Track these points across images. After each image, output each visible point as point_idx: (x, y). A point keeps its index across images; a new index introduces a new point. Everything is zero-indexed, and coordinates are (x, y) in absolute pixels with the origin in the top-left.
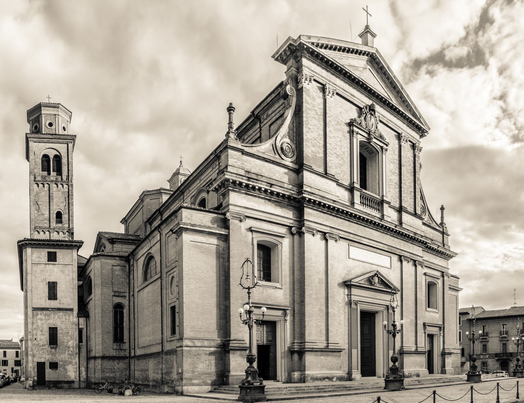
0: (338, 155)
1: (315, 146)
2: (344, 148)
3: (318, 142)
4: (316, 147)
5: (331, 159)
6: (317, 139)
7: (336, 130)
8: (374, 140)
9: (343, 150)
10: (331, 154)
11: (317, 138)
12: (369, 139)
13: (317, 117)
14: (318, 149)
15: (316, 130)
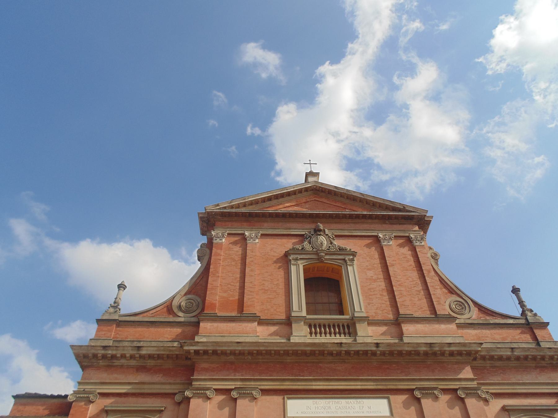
0: (266, 290)
1: (227, 291)
2: (278, 280)
3: (233, 285)
4: (229, 292)
5: (250, 297)
6: (232, 284)
7: (264, 267)
8: (327, 257)
9: (275, 283)
10: (251, 292)
11: (232, 282)
12: (320, 259)
13: (233, 263)
14: (231, 293)
15: (232, 275)
